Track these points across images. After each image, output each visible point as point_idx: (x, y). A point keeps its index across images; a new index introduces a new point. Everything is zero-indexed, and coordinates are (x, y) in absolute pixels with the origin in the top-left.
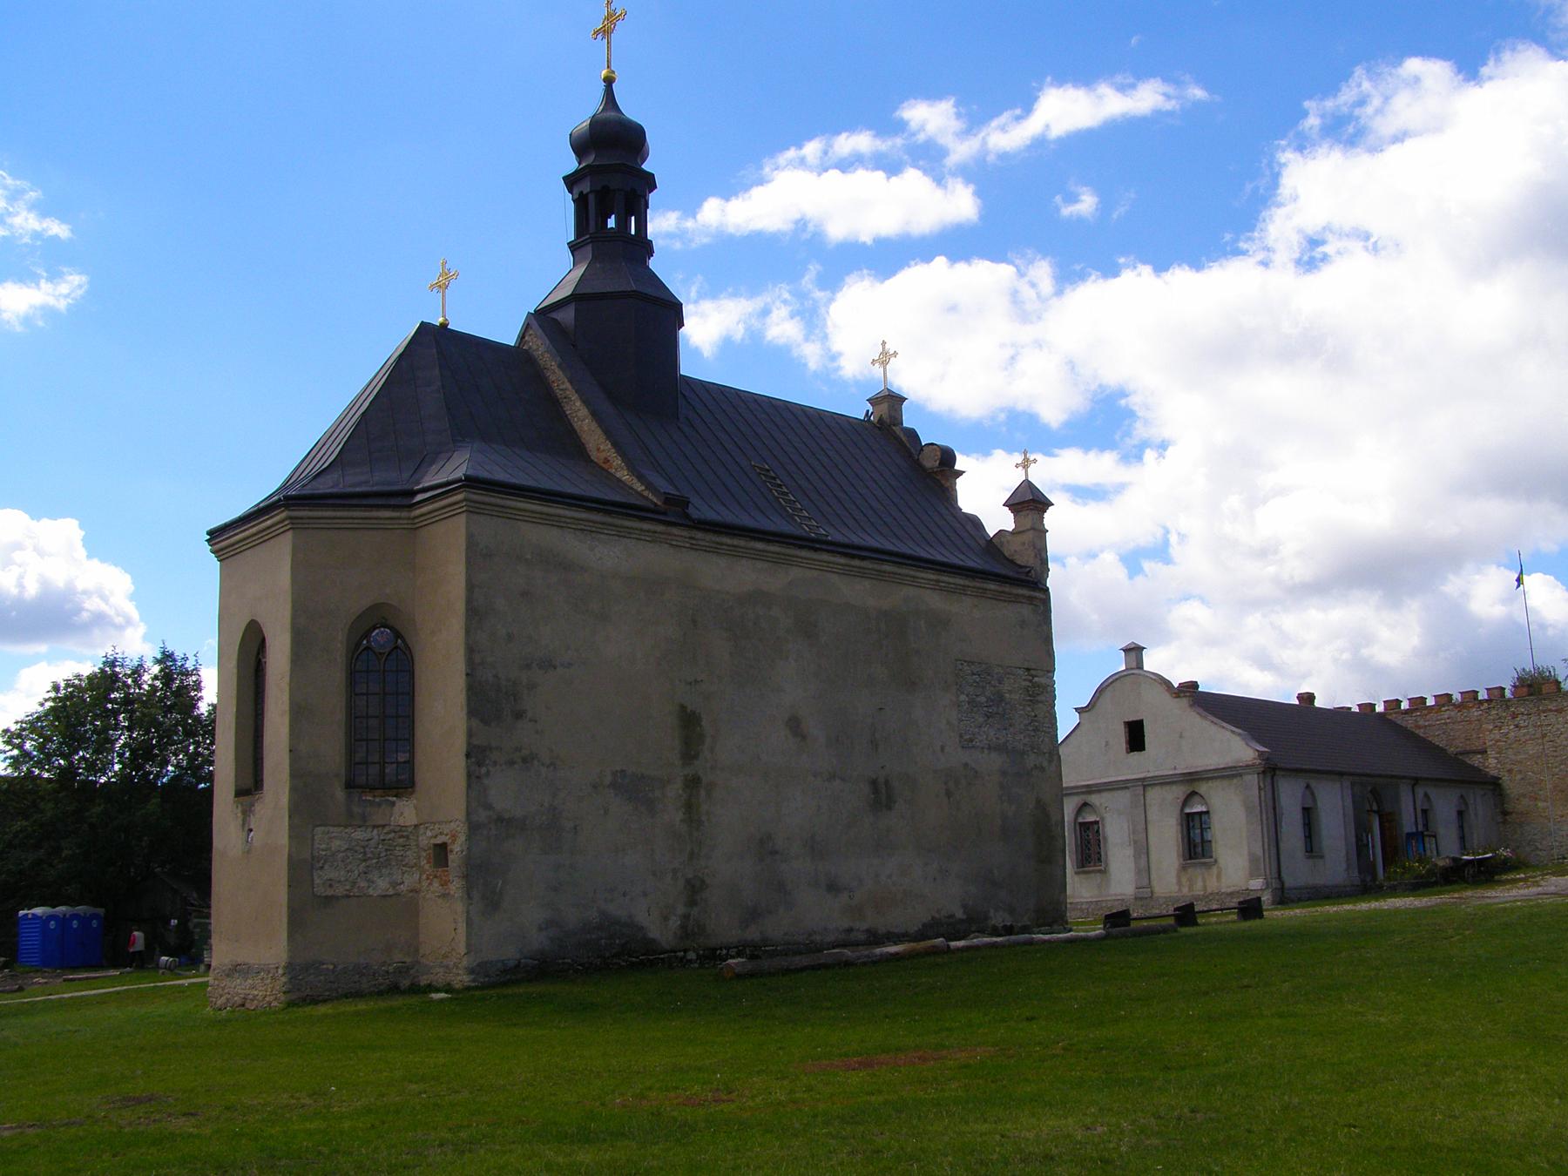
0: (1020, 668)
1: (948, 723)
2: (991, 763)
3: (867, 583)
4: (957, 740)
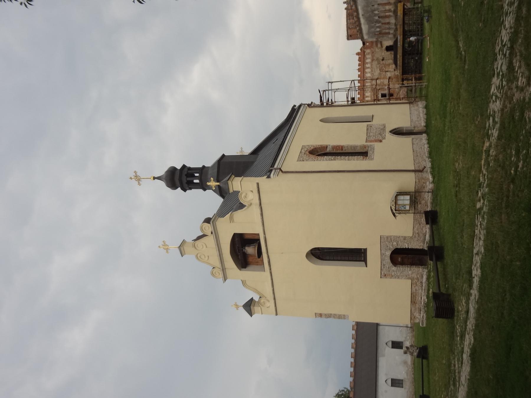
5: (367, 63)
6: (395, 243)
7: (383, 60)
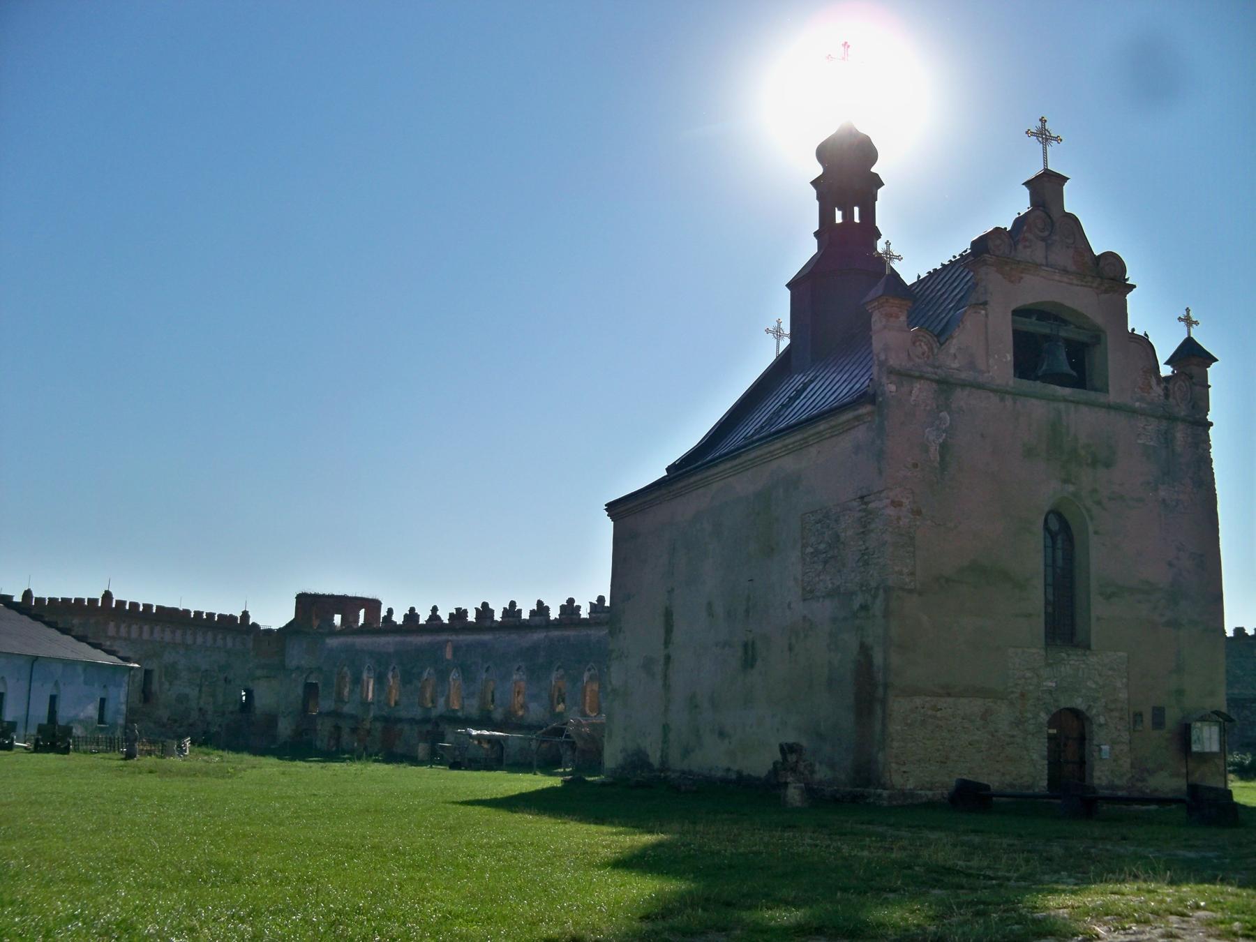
5: (224, 639)
6: (1102, 720)
7: (226, 679)
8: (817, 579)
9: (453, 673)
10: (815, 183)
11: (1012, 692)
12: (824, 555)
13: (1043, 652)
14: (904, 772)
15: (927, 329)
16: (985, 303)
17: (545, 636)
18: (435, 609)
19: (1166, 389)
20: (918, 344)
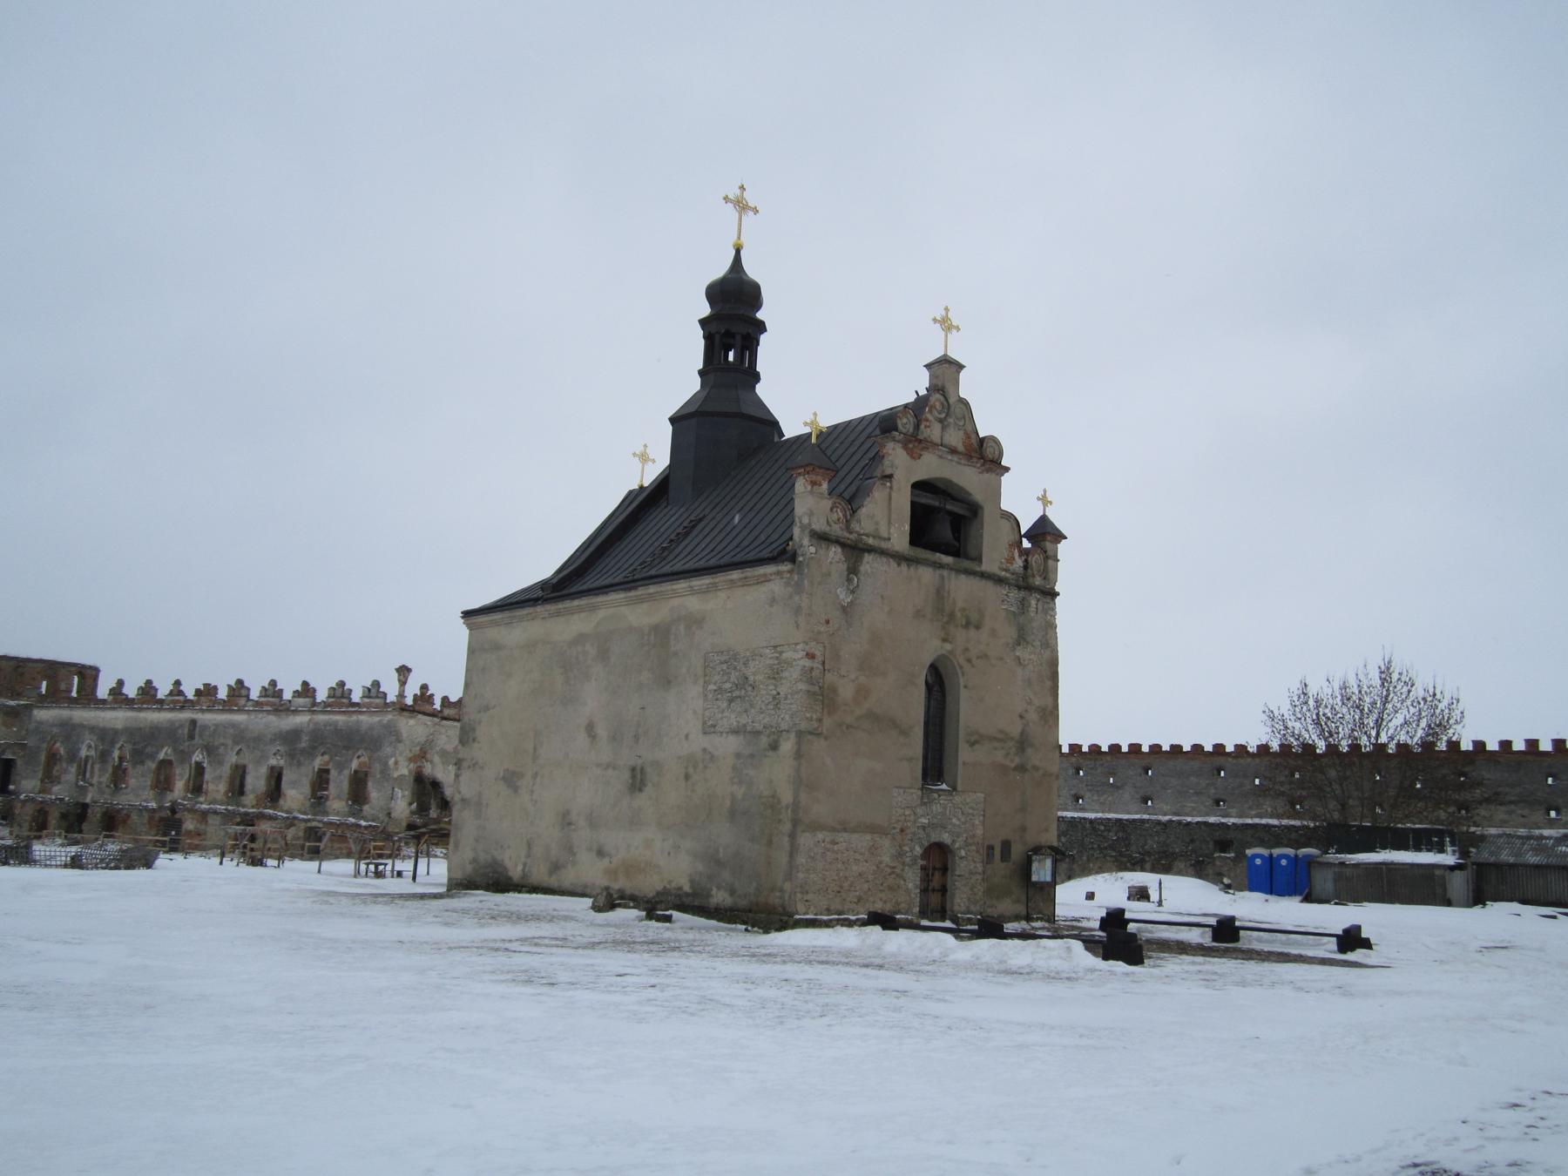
0: (767, 647)
1: (695, 712)
2: (727, 746)
3: (645, 606)
4: (700, 727)
6: (963, 853)
8: (720, 715)
9: (196, 754)
10: (704, 323)
11: (894, 828)
12: (730, 694)
13: (920, 792)
14: (807, 901)
15: (840, 495)
16: (890, 477)
17: (310, 720)
18: (178, 683)
19: (1026, 561)
20: (835, 510)
